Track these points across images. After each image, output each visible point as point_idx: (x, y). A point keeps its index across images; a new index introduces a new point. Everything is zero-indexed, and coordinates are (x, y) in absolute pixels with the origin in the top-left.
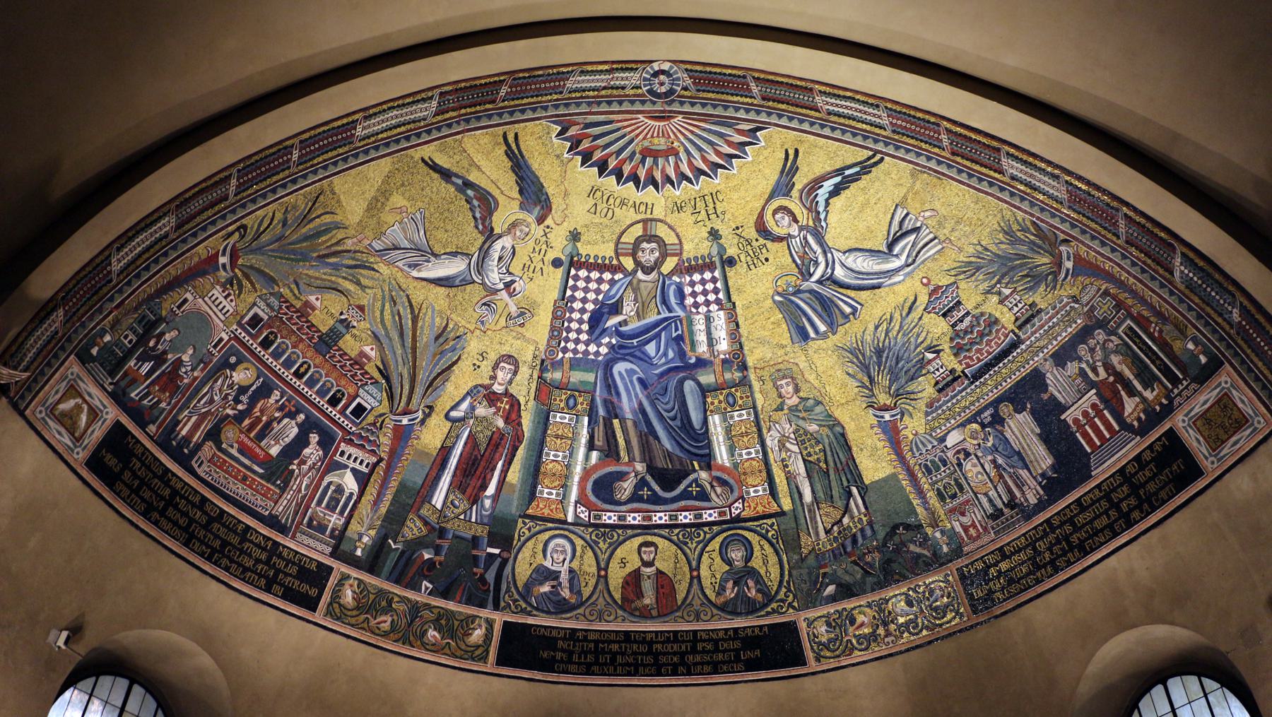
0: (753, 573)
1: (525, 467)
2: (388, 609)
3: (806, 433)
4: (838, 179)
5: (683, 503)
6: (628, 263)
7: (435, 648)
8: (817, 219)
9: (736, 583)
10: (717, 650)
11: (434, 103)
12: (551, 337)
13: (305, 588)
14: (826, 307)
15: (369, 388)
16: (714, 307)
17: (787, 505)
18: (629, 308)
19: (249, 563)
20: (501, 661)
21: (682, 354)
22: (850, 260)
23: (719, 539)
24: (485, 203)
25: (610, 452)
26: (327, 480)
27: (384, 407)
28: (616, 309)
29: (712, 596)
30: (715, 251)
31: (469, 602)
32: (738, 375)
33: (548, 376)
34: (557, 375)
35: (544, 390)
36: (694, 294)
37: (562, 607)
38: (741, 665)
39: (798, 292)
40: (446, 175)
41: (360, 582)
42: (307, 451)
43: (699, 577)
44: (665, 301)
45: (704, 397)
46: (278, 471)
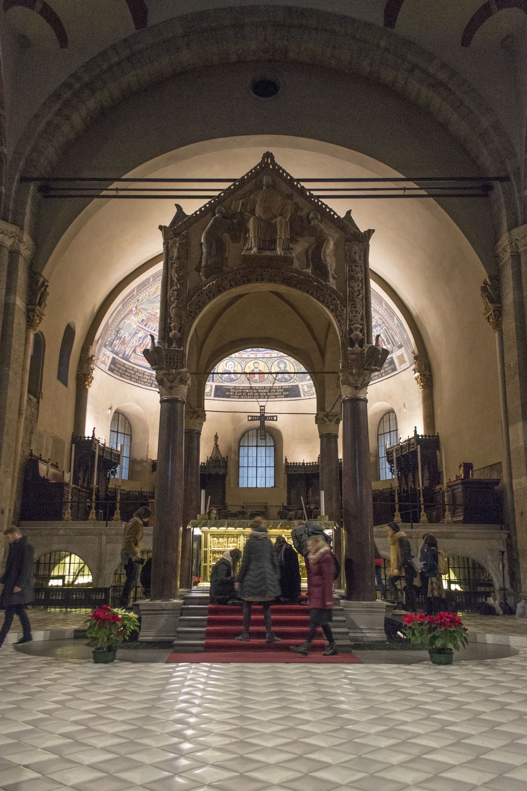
10: (276, 392)
19: (145, 380)
20: (215, 396)
38: (283, 396)
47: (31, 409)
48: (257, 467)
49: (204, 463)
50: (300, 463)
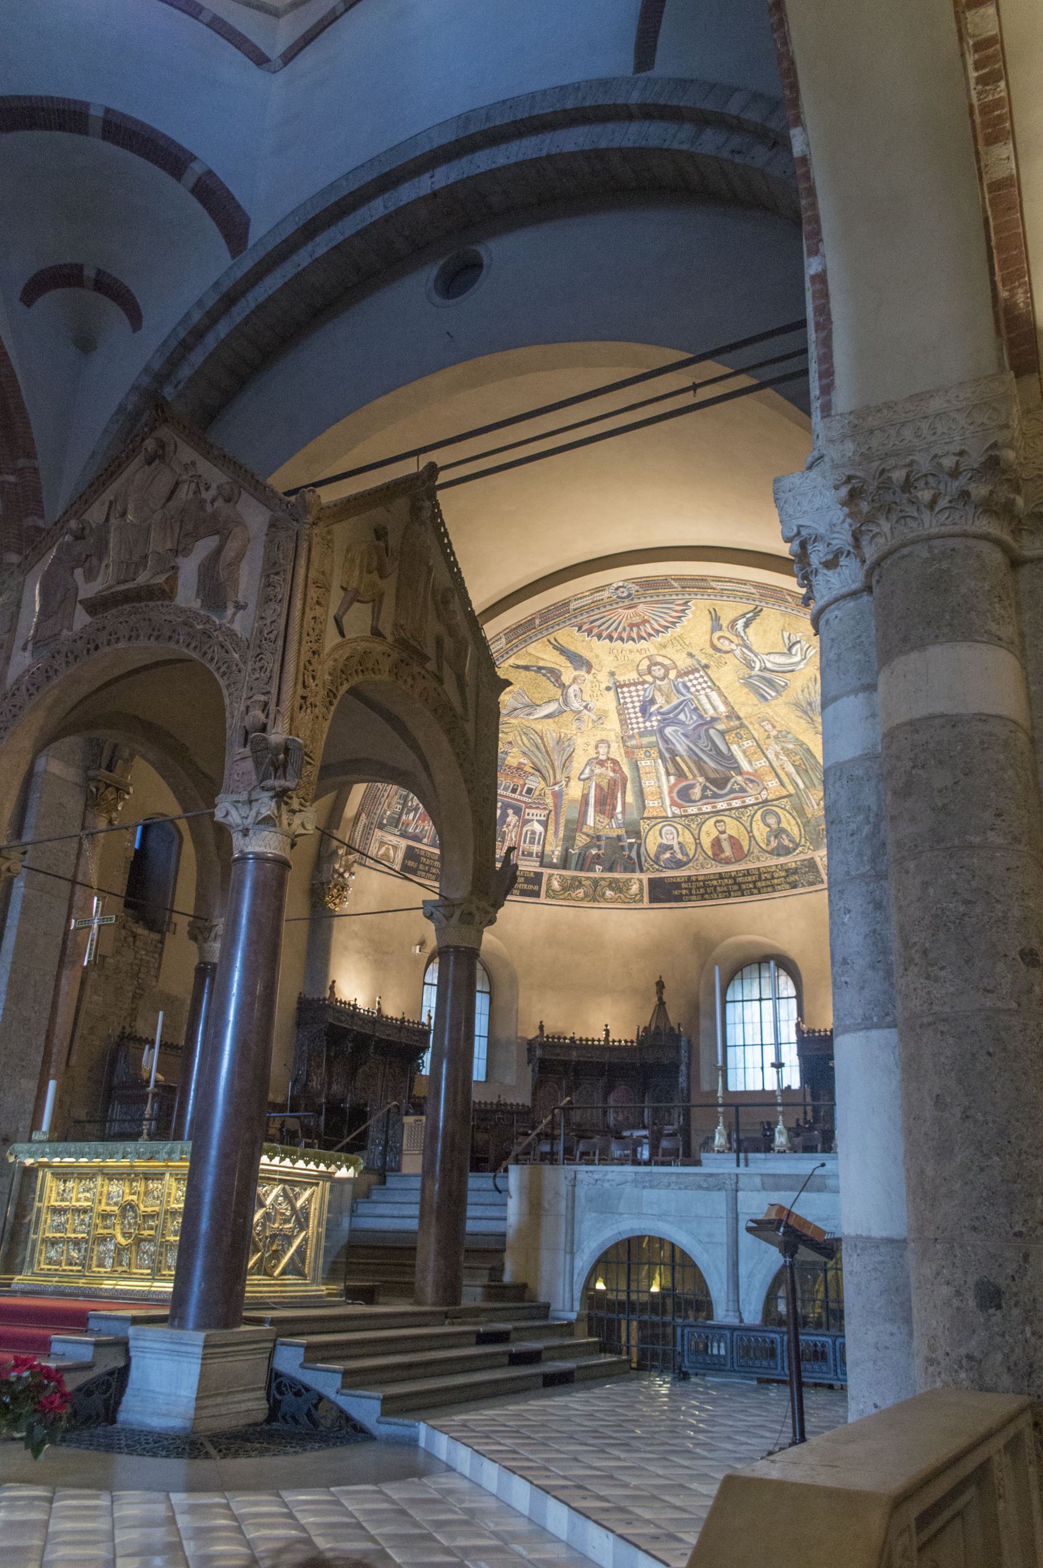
0: (783, 831)
1: (635, 793)
2: (581, 885)
3: (788, 749)
4: (744, 620)
5: (732, 796)
6: (649, 678)
7: (612, 900)
8: (743, 640)
9: (776, 837)
10: (773, 878)
11: (503, 640)
12: (622, 725)
13: (531, 887)
14: (770, 683)
15: (531, 778)
16: (708, 690)
17: (792, 791)
18: (660, 700)
20: (651, 901)
21: (701, 717)
22: (772, 658)
23: (759, 813)
24: (554, 675)
25: (680, 774)
26: (525, 829)
27: (543, 784)
28: (652, 701)
29: (764, 846)
30: (695, 663)
31: (626, 870)
32: (737, 723)
33: (628, 744)
34: (634, 742)
35: (629, 753)
36: (694, 686)
37: (679, 864)
39: (750, 677)
40: (526, 668)
41: (560, 876)
42: (509, 819)
43: (753, 836)
44: (679, 692)
45: (724, 736)
47: (136, 952)
48: (762, 1045)
49: (632, 1042)
50: (826, 1031)
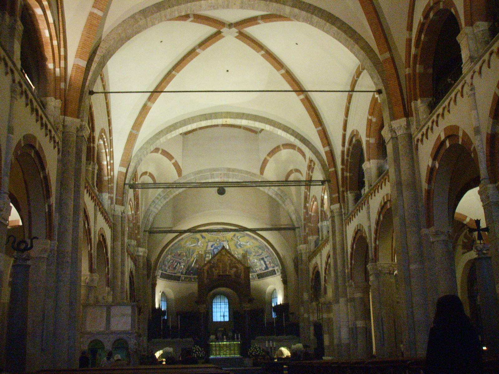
14: (240, 246)
18: (216, 245)
24: (198, 239)
40: (193, 238)
46: (175, 268)
